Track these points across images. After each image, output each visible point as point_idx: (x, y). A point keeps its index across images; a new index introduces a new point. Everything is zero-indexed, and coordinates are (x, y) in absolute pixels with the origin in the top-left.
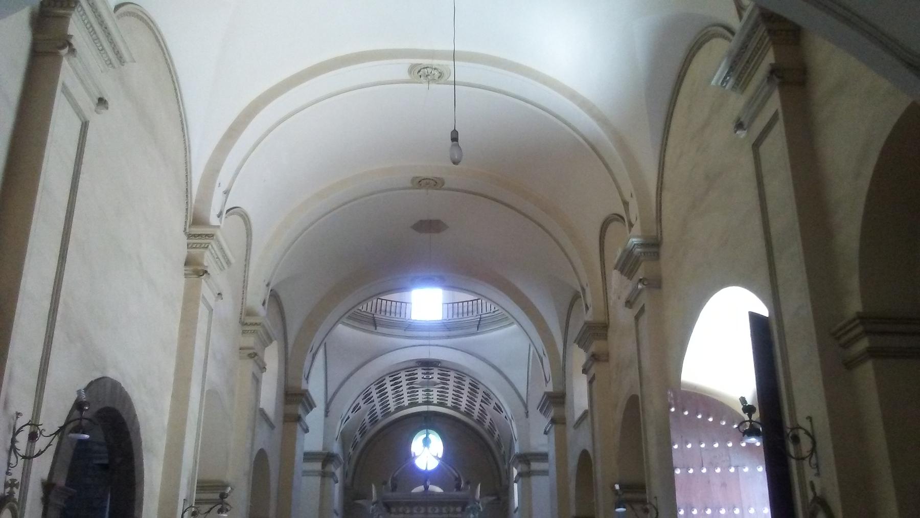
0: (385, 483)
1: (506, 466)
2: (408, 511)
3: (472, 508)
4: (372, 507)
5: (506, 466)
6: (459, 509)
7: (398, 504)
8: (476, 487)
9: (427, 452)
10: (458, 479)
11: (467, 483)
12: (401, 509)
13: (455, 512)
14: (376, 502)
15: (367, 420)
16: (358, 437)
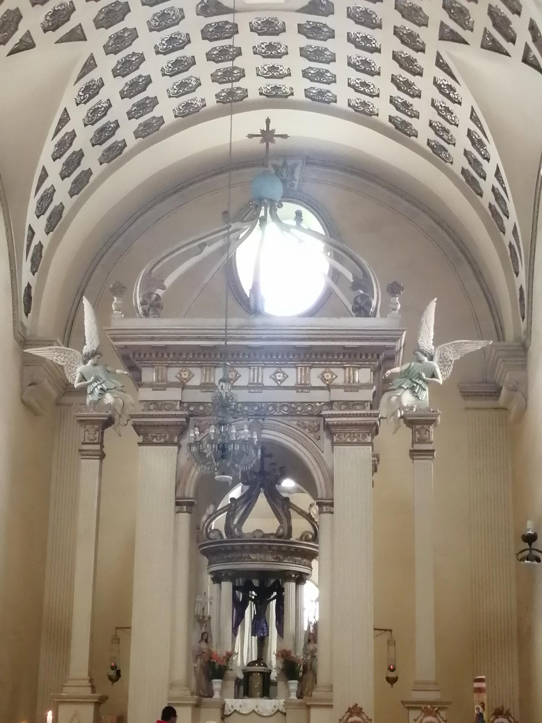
0: (120, 289)
1: (522, 280)
2: (196, 381)
3: (406, 374)
4: (80, 368)
5: (522, 280)
6: (363, 375)
7: (162, 355)
8: (421, 312)
9: (286, 267)
10: (361, 283)
11: (394, 289)
12: (173, 374)
13: (351, 386)
14: (93, 354)
15: (84, 136)
16: (62, 188)
